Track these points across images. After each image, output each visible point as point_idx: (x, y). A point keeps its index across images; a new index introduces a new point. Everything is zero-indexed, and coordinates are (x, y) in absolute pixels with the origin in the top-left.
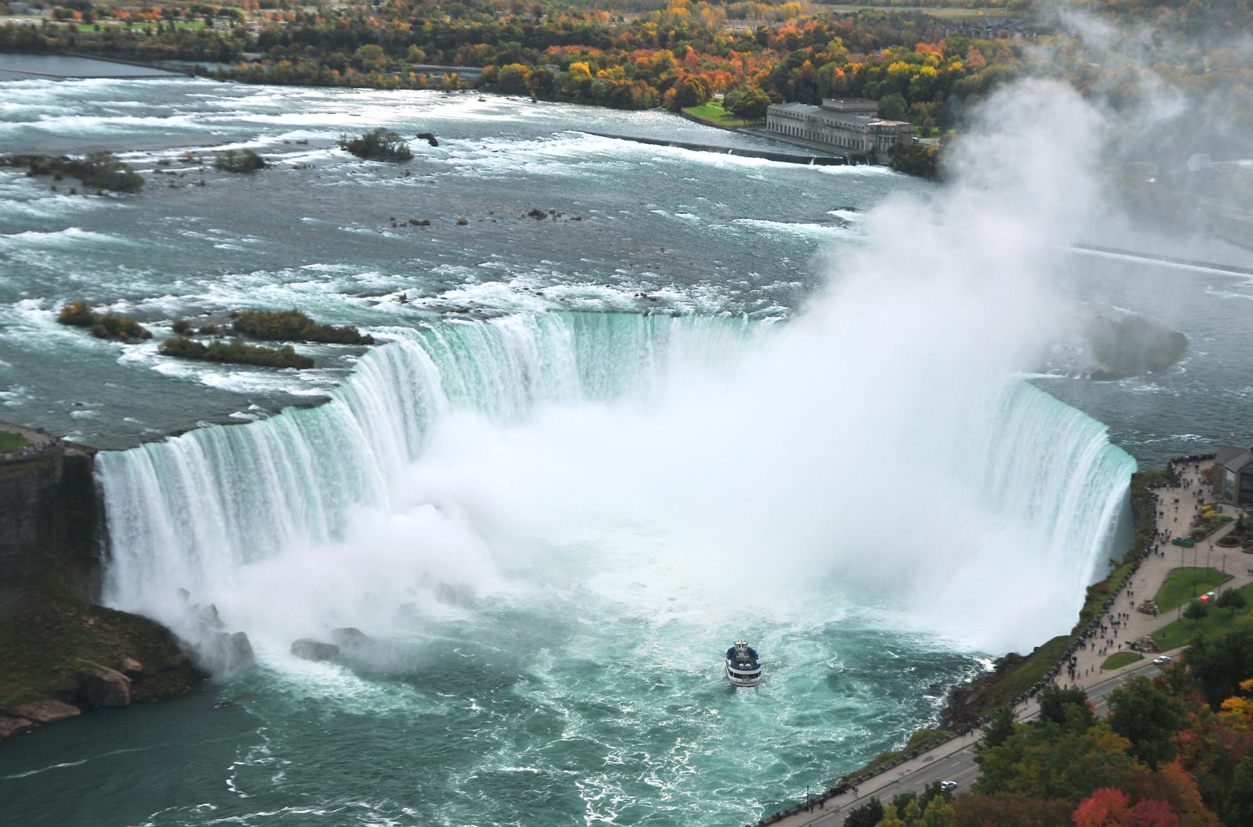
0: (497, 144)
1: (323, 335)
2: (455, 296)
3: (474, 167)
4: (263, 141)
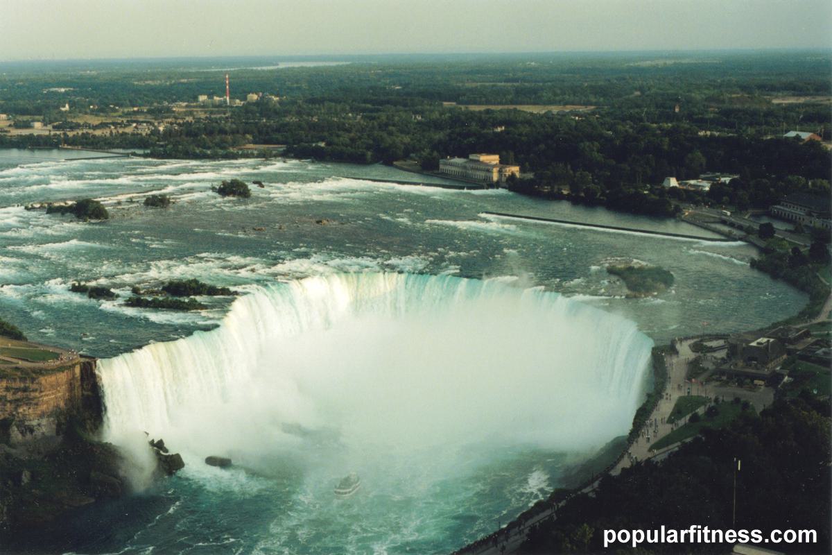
0: (297, 185)
1: (212, 291)
2: (280, 268)
3: (285, 198)
4: (170, 189)
